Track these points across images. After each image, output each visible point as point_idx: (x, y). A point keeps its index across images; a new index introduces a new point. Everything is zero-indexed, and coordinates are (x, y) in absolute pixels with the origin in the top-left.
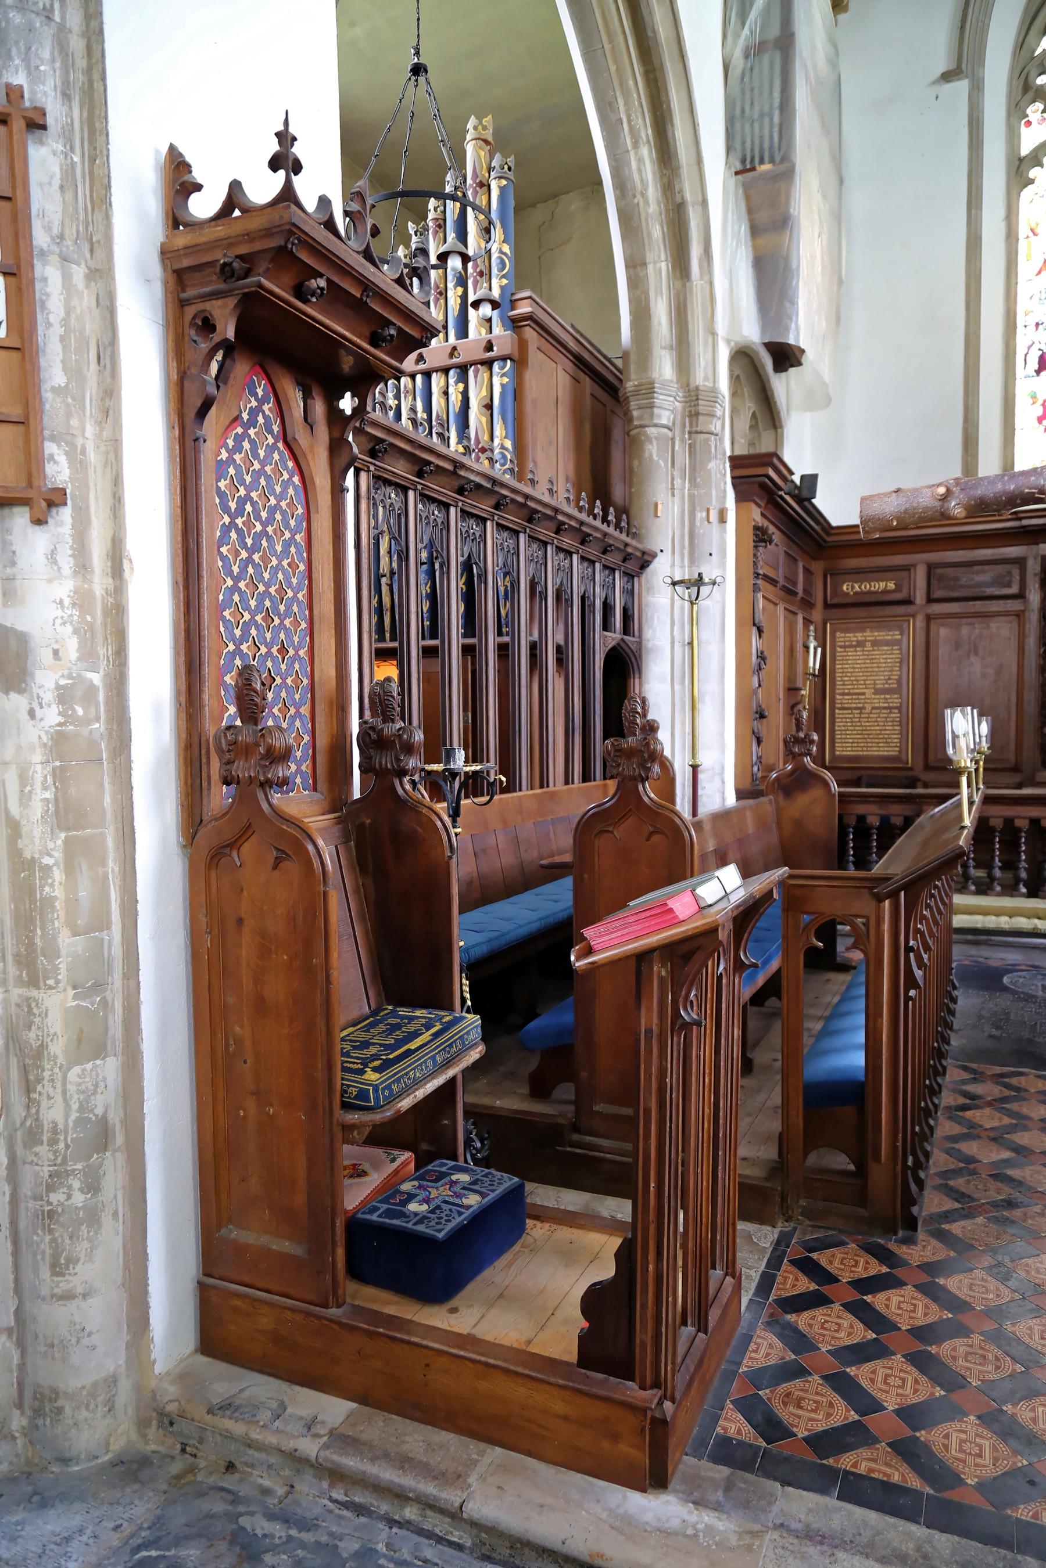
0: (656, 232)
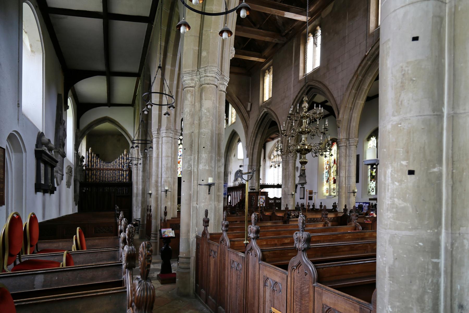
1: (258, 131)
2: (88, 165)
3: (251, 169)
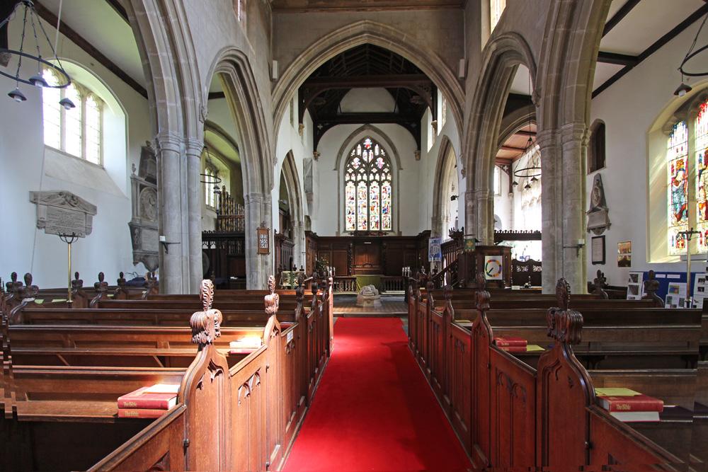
0: (295, 201)
1: (482, 112)
2: (221, 212)
3: (473, 200)
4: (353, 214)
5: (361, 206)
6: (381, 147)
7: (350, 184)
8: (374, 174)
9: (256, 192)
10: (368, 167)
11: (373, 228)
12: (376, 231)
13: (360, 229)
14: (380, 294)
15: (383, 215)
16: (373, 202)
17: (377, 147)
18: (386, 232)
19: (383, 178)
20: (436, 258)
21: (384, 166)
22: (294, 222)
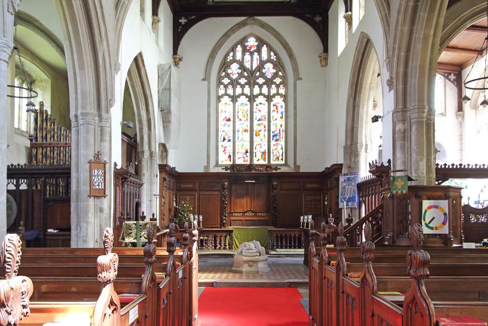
0: (145, 123)
2: (36, 138)
3: (403, 121)
4: (229, 141)
5: (241, 130)
6: (270, 49)
7: (226, 99)
8: (261, 86)
9: (88, 111)
10: (251, 76)
11: (259, 160)
12: (262, 166)
13: (239, 162)
14: (267, 253)
15: (273, 143)
16: (259, 125)
17: (264, 49)
18: (276, 167)
19: (274, 91)
20: (350, 204)
21: (275, 75)
22: (143, 152)
